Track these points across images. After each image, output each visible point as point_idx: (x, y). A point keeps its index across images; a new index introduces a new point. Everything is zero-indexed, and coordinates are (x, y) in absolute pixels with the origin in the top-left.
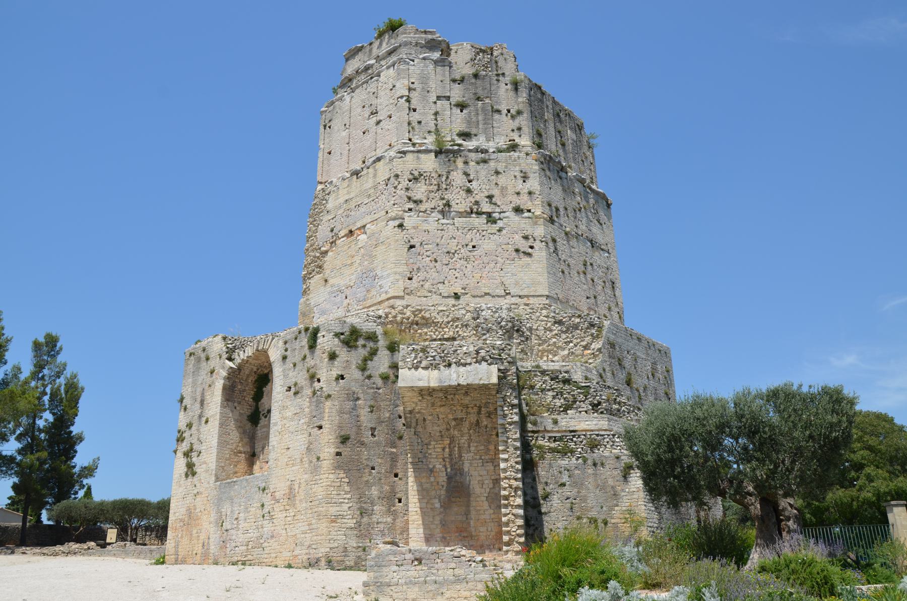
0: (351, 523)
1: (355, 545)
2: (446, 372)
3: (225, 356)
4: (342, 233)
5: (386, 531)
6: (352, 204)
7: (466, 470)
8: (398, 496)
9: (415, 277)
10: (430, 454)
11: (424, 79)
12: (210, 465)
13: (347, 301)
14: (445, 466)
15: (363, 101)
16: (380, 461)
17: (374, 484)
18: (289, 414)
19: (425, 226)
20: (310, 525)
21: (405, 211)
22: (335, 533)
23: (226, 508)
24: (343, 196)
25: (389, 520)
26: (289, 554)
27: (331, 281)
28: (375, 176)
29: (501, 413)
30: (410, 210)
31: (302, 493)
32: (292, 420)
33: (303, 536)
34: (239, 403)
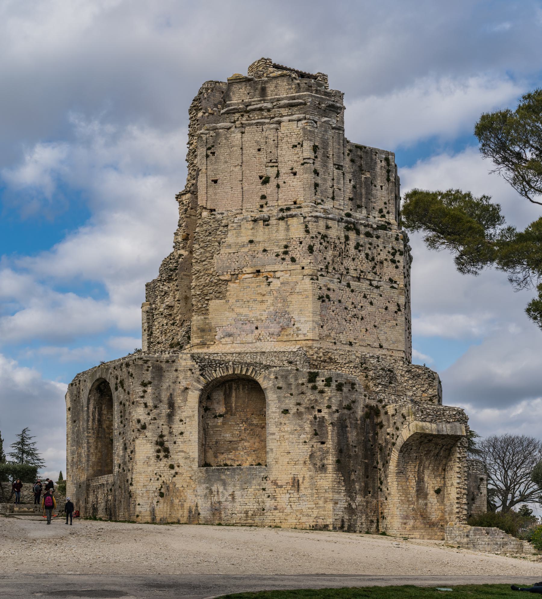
4: (249, 270)
9: (325, 327)
13: (259, 331)
15: (257, 142)
16: (359, 467)
17: (357, 481)
24: (246, 234)
26: (296, 521)
27: (237, 310)
28: (288, 229)
29: (459, 451)
30: (321, 269)
31: (307, 483)
32: (292, 433)
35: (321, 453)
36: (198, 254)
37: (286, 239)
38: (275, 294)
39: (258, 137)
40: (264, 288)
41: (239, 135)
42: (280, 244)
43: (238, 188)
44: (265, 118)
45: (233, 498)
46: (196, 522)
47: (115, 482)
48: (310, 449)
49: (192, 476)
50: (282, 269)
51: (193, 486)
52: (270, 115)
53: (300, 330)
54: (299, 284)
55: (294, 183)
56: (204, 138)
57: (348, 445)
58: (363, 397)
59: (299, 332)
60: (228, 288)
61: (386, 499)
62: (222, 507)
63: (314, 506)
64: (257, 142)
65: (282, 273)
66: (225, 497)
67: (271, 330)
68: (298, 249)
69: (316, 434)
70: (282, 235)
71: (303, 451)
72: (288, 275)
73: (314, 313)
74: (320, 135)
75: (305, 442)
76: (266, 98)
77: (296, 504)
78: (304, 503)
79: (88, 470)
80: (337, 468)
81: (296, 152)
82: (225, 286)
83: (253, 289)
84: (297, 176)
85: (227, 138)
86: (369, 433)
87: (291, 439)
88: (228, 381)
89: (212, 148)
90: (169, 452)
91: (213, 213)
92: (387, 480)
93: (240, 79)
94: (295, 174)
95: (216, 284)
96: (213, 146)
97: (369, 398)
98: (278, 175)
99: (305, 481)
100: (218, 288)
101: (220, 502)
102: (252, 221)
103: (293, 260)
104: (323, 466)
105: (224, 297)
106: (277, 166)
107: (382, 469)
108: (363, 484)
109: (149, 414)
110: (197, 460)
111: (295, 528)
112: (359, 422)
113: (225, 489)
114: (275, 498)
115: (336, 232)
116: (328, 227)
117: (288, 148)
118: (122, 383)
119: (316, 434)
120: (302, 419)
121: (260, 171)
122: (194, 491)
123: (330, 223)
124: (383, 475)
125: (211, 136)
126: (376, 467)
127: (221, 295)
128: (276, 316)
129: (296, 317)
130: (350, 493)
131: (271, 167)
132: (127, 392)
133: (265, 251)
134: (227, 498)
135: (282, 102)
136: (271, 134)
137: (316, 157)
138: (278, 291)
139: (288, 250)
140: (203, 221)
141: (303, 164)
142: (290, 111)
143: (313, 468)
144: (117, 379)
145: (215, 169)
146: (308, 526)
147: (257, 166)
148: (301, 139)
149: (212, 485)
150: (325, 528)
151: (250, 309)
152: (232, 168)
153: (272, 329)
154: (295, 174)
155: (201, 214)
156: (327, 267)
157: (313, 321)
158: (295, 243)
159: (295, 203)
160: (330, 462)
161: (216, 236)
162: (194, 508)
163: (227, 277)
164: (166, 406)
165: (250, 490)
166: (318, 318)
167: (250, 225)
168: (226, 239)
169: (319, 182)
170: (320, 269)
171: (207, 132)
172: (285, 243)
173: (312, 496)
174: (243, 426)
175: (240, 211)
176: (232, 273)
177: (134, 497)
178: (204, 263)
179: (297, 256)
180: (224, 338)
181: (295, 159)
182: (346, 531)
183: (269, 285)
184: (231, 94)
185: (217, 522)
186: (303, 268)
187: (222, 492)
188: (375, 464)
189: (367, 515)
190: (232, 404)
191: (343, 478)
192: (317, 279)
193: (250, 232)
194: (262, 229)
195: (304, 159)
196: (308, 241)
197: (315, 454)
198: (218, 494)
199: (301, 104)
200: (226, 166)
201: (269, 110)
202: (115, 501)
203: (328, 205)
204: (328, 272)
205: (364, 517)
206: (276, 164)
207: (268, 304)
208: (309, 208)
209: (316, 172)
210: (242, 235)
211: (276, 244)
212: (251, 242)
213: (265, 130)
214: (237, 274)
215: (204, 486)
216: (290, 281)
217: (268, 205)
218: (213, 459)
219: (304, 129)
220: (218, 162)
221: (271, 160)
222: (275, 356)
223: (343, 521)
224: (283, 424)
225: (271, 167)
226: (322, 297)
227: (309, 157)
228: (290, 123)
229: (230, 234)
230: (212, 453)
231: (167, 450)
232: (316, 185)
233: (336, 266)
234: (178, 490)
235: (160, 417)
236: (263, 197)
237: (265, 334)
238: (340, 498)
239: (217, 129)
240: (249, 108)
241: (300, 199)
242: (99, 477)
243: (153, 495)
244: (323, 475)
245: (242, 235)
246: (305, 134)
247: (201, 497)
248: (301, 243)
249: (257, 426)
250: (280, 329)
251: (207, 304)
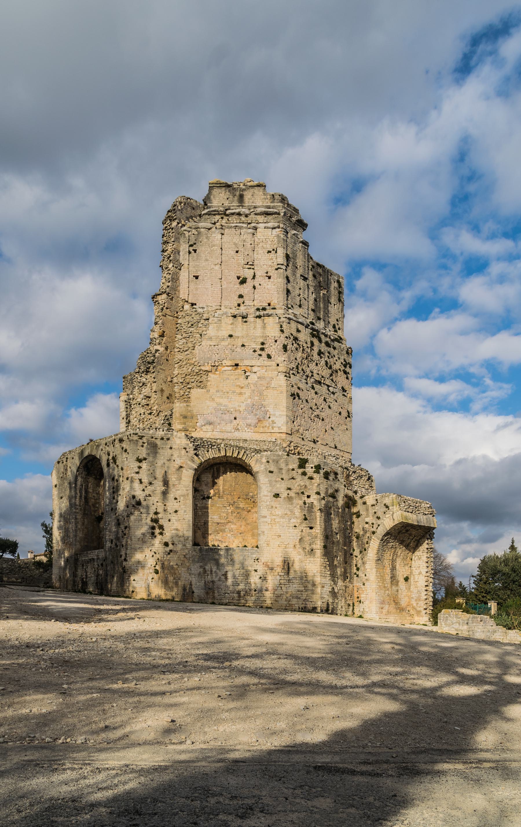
3: (192, 452)
4: (229, 363)
15: (235, 244)
18: (279, 512)
21: (290, 369)
26: (286, 603)
28: (264, 327)
32: (282, 517)
35: (310, 538)
36: (180, 343)
37: (263, 337)
38: (253, 388)
39: (236, 239)
40: (242, 381)
41: (220, 236)
42: (257, 340)
43: (218, 285)
44: (243, 223)
45: (226, 578)
46: (191, 600)
47: (106, 557)
48: (300, 533)
49: (186, 554)
50: (259, 365)
51: (187, 564)
52: (247, 220)
53: (275, 423)
54: (275, 379)
55: (269, 286)
56: (187, 235)
57: (332, 531)
58: (343, 487)
59: (274, 425)
60: (209, 379)
61: (364, 584)
63: (303, 589)
64: (235, 244)
65: (259, 368)
66: (218, 577)
67: (249, 421)
68: (273, 347)
69: (306, 519)
70: (258, 332)
71: (293, 535)
72: (264, 370)
73: (288, 408)
74: (291, 246)
75: (295, 526)
76: (244, 204)
77: (286, 586)
79: (75, 545)
80: (323, 553)
81: (270, 257)
82: (205, 376)
83: (232, 381)
84: (271, 280)
85: (207, 238)
86: (348, 522)
87: (281, 523)
88: (216, 464)
89: (194, 246)
90: (163, 530)
91: (194, 306)
92: (365, 567)
93: (220, 183)
94: (269, 278)
95: (197, 374)
96: (195, 244)
97: (348, 489)
98: (254, 277)
100: (198, 378)
101: (213, 582)
102: (232, 316)
103: (269, 356)
104: (312, 550)
105: (205, 387)
106: (253, 269)
107: (359, 557)
108: (343, 570)
109: (144, 490)
110: (190, 538)
111: (286, 609)
112: (340, 510)
113: (218, 568)
115: (304, 336)
116: (298, 331)
117: (263, 252)
118: (114, 459)
119: (306, 519)
121: (238, 272)
122: (188, 569)
123: (300, 327)
124: (360, 562)
125: (194, 234)
126: (352, 554)
127: (201, 385)
128: (253, 408)
130: (333, 576)
131: (248, 268)
132: (120, 467)
133: (243, 346)
134: (220, 577)
135: (259, 210)
136: (249, 238)
137: (288, 265)
138: (255, 385)
139: (264, 347)
140: (186, 313)
141: (277, 269)
142: (266, 219)
143: (302, 552)
144: (109, 455)
145: (197, 265)
146: (297, 608)
147: (235, 267)
148: (275, 246)
149: (206, 564)
150: (314, 610)
151: (229, 400)
152: (213, 266)
153: (250, 421)
154: (269, 278)
155: (183, 307)
156: (297, 367)
158: (270, 342)
159: (269, 305)
160: (318, 547)
161: (198, 328)
162: (188, 586)
163: (208, 368)
164: (161, 484)
166: (290, 414)
167: (230, 320)
168: (208, 332)
169: (290, 288)
170: (292, 368)
171: (189, 229)
172: (262, 340)
174: (230, 509)
175: (219, 307)
176: (212, 365)
177: (129, 573)
178: (186, 353)
179: (273, 354)
180: (205, 425)
181: (270, 263)
182: (330, 614)
183: (247, 378)
184: (212, 197)
185: (210, 601)
186: (278, 365)
187: (215, 572)
188: (352, 551)
189: (346, 599)
190: (219, 487)
191: (328, 563)
192: (290, 377)
193: (230, 327)
194: (240, 325)
195: (278, 264)
196: (282, 340)
197: (304, 539)
198: (211, 573)
199: (276, 213)
200: (207, 263)
201: (246, 216)
202: (107, 576)
203: (297, 311)
204: (298, 373)
206: (252, 267)
208: (283, 310)
209: (287, 278)
210: (222, 329)
211: (254, 340)
212: (231, 336)
213: (242, 233)
215: (198, 565)
216: (266, 376)
217: (245, 304)
218: (202, 539)
219: (278, 236)
220: (200, 259)
222: (256, 445)
223: (328, 604)
224: (274, 508)
225: (248, 268)
226: (294, 394)
227: (282, 263)
228: (266, 229)
229: (211, 327)
230: (201, 533)
231: (161, 527)
232: (288, 291)
233: (304, 368)
234: (172, 567)
235: (155, 494)
236: (241, 296)
238: (326, 582)
239: (199, 228)
240: (228, 212)
241: (274, 302)
242: (89, 552)
243: (148, 571)
244: (312, 559)
245: (222, 329)
246: (279, 242)
247: (195, 575)
248: (276, 341)
249: (243, 509)
250: (257, 421)
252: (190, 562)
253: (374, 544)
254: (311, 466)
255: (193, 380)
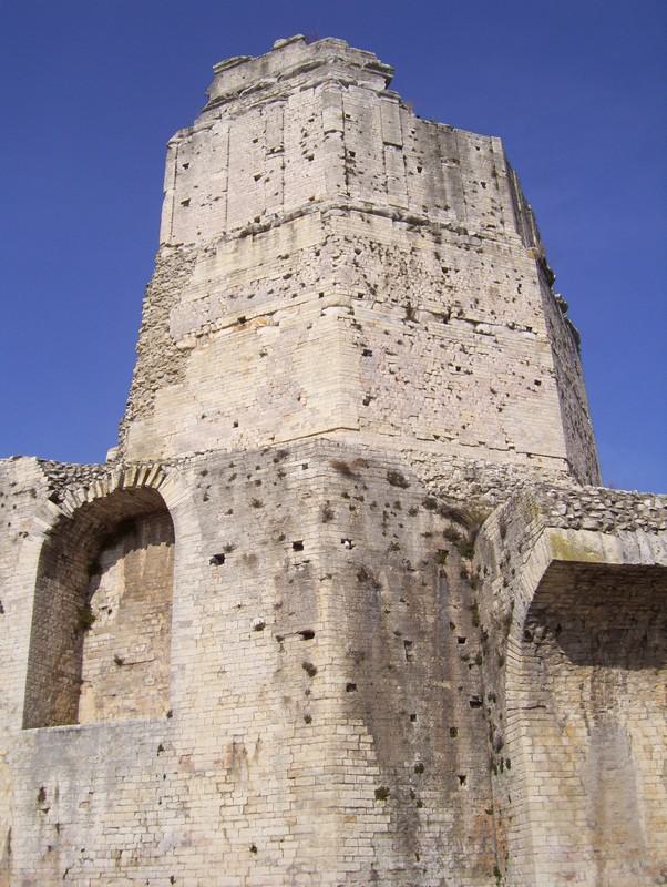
0: (383, 823)
1: (391, 867)
2: (630, 539)
3: (45, 493)
5: (445, 840)
6: (247, 278)
7: (622, 723)
8: (463, 771)
10: (559, 693)
11: (365, 115)
12: (11, 694)
14: (585, 717)
18: (221, 606)
19: (385, 326)
20: (290, 825)
22: (354, 843)
23: (55, 781)
25: (448, 817)
32: (230, 617)
33: (276, 845)
34: (63, 582)
62: (62, 841)
78: (259, 823)
99: (260, 754)
110: (21, 709)
114: (184, 809)
120: (256, 575)
129: (308, 388)
151: (225, 391)
154: (311, 158)
157: (344, 391)
165: (127, 786)
166: (354, 385)
173: (279, 801)
186: (321, 295)
191: (370, 739)
205: (448, 860)
207: (259, 372)
214: (207, 334)
221: (272, 150)
237: (250, 434)
248: (318, 254)
251: (153, 398)
252: (16, 772)
253: (515, 655)
254: (303, 462)
255: (160, 374)
